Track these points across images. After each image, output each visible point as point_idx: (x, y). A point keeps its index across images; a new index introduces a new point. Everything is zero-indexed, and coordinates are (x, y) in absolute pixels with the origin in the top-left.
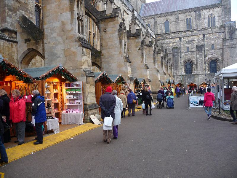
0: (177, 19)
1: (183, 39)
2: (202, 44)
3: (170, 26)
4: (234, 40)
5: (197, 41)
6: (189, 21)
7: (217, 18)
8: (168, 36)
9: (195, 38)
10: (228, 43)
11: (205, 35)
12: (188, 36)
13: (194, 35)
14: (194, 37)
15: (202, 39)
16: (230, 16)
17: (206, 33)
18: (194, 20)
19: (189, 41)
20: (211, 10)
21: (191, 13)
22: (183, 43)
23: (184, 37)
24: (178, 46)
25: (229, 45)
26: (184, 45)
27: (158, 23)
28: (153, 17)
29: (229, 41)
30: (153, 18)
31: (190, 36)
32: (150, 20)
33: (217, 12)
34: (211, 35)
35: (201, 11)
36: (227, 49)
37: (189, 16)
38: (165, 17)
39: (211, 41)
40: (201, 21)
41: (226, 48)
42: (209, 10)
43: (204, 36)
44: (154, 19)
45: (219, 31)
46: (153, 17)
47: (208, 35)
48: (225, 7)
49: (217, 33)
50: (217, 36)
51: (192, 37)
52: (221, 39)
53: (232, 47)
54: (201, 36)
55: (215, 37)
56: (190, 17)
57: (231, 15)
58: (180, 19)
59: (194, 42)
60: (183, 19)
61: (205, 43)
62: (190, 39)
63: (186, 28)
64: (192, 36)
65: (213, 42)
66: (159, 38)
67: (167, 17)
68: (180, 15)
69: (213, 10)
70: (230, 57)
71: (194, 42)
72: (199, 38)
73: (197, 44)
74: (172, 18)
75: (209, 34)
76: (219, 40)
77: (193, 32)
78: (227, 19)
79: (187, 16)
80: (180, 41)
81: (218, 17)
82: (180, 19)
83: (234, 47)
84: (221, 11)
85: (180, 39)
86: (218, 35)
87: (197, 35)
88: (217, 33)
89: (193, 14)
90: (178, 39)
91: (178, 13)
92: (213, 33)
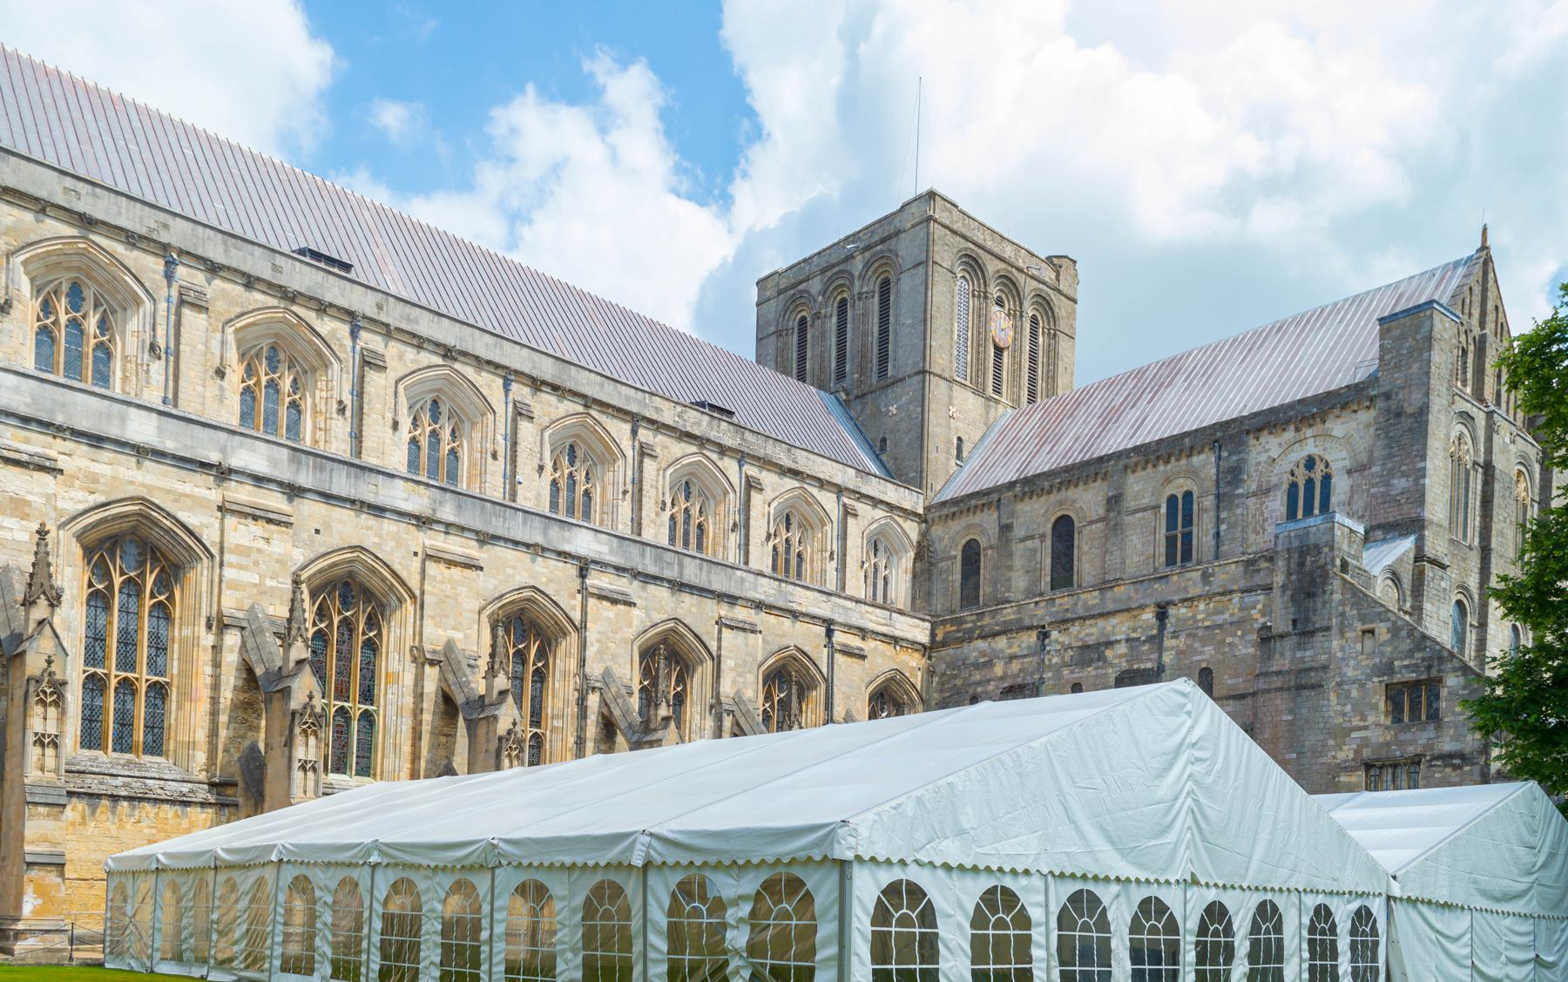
0: (1114, 502)
1: (1054, 634)
2: (1149, 665)
3: (1076, 551)
4: (1319, 637)
5: (1122, 649)
6: (1180, 511)
7: (1341, 485)
8: (987, 620)
9: (1119, 627)
10: (1285, 657)
11: (1172, 611)
12: (1084, 619)
13: (1110, 607)
14: (1114, 621)
15: (1154, 632)
16: (1421, 465)
17: (1175, 598)
18: (1209, 501)
19: (1085, 647)
20: (1309, 432)
21: (1195, 460)
22: (1055, 660)
23: (1063, 623)
24: (1029, 680)
25: (1288, 672)
26: (1057, 669)
27: (1018, 532)
28: (995, 497)
29: (1288, 643)
30: (991, 503)
31: (1093, 617)
32: (977, 519)
33: (1348, 439)
34: (1202, 606)
35: (1252, 441)
36: (1272, 695)
37: (1182, 480)
38: (1054, 497)
39: (1197, 645)
40: (1239, 511)
41: (1268, 691)
42: (1297, 430)
43: (1162, 616)
44: (998, 507)
45: (1243, 584)
46: (995, 497)
47: (1183, 610)
48: (1393, 403)
49: (1231, 592)
50: (1232, 615)
51: (1101, 623)
52: (1251, 631)
53: (1300, 688)
54: (1148, 616)
55: (1219, 619)
56: (1188, 485)
57: (1423, 458)
58: (1131, 504)
59: (1109, 653)
60: (1146, 501)
61: (1167, 658)
62: (1091, 632)
63: (1163, 559)
64: (1102, 615)
65: (1209, 650)
66: (946, 634)
67: (1063, 494)
68: (1131, 478)
69: (1319, 428)
70: (1291, 748)
71: (1109, 653)
72: (1134, 630)
73: (1125, 666)
74: (1087, 501)
75: (1191, 599)
76: (1243, 635)
77: (1109, 594)
78: (1400, 484)
79: (1168, 480)
80: (1043, 647)
81: (1349, 472)
82: (1132, 505)
83: (1313, 687)
84: (1372, 430)
85: (1044, 635)
86: (1241, 609)
87: (1128, 610)
88: (1231, 592)
89: (1205, 462)
90: (1031, 638)
91: (1122, 463)
92: (1209, 597)
